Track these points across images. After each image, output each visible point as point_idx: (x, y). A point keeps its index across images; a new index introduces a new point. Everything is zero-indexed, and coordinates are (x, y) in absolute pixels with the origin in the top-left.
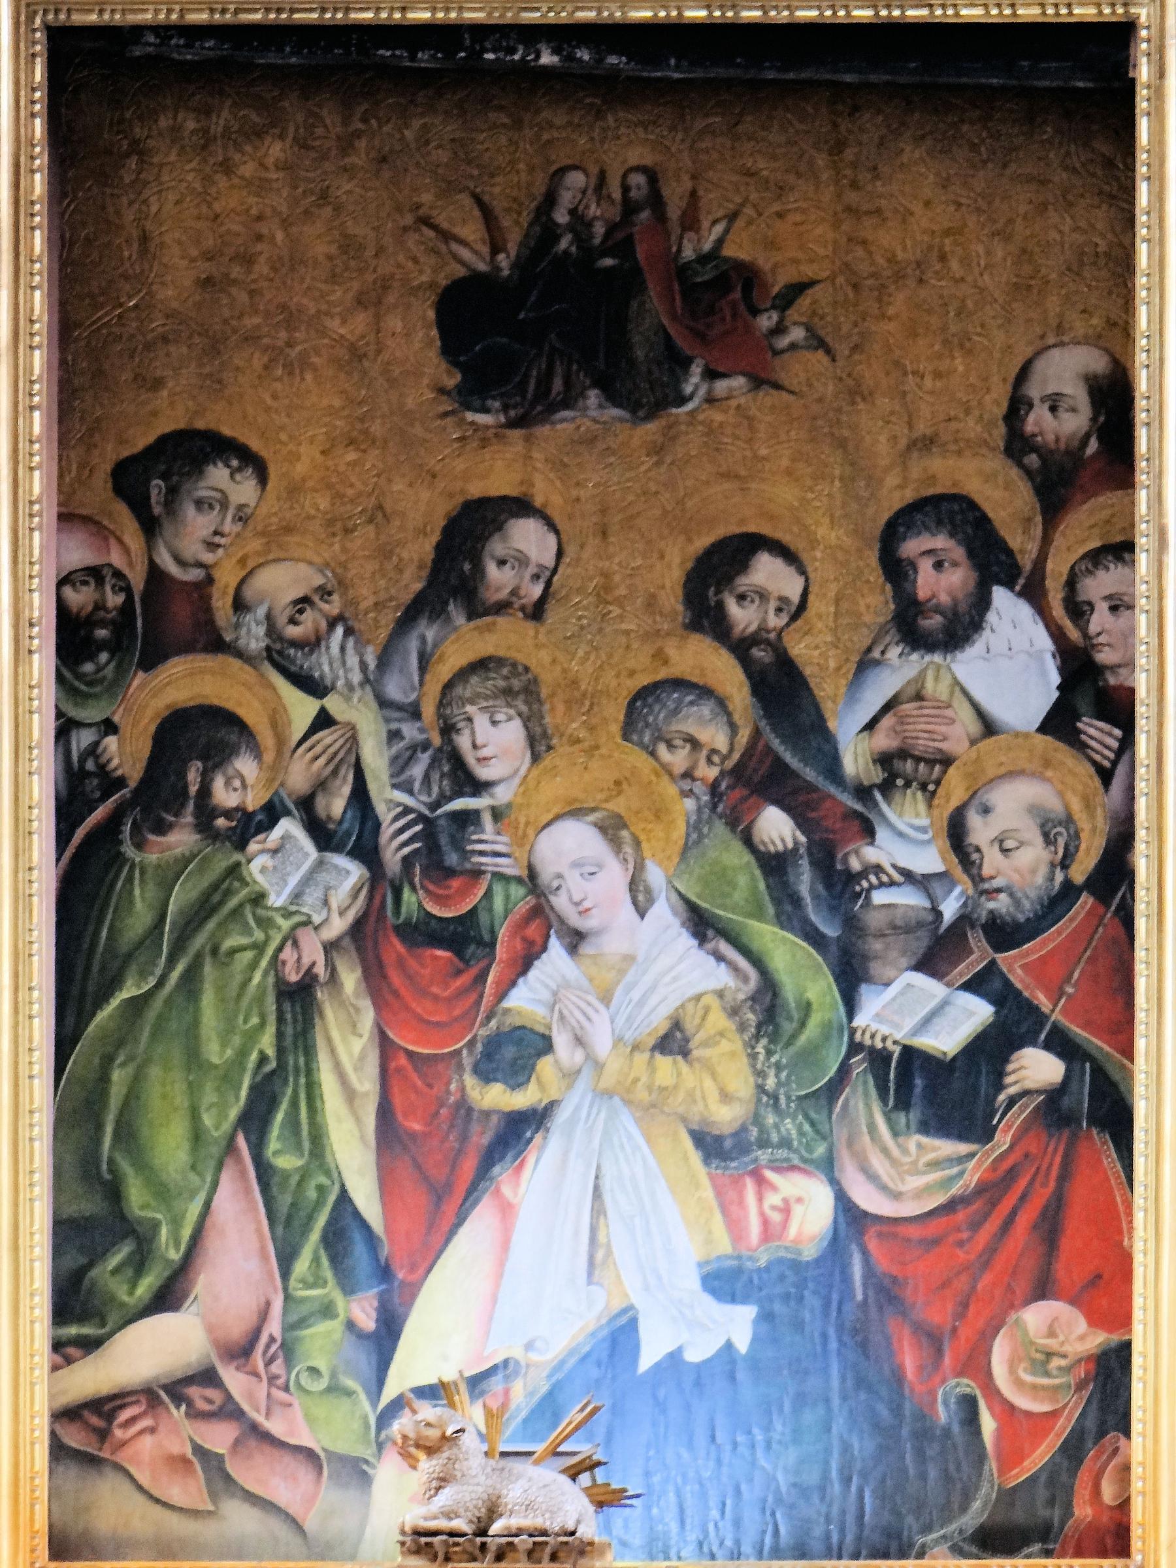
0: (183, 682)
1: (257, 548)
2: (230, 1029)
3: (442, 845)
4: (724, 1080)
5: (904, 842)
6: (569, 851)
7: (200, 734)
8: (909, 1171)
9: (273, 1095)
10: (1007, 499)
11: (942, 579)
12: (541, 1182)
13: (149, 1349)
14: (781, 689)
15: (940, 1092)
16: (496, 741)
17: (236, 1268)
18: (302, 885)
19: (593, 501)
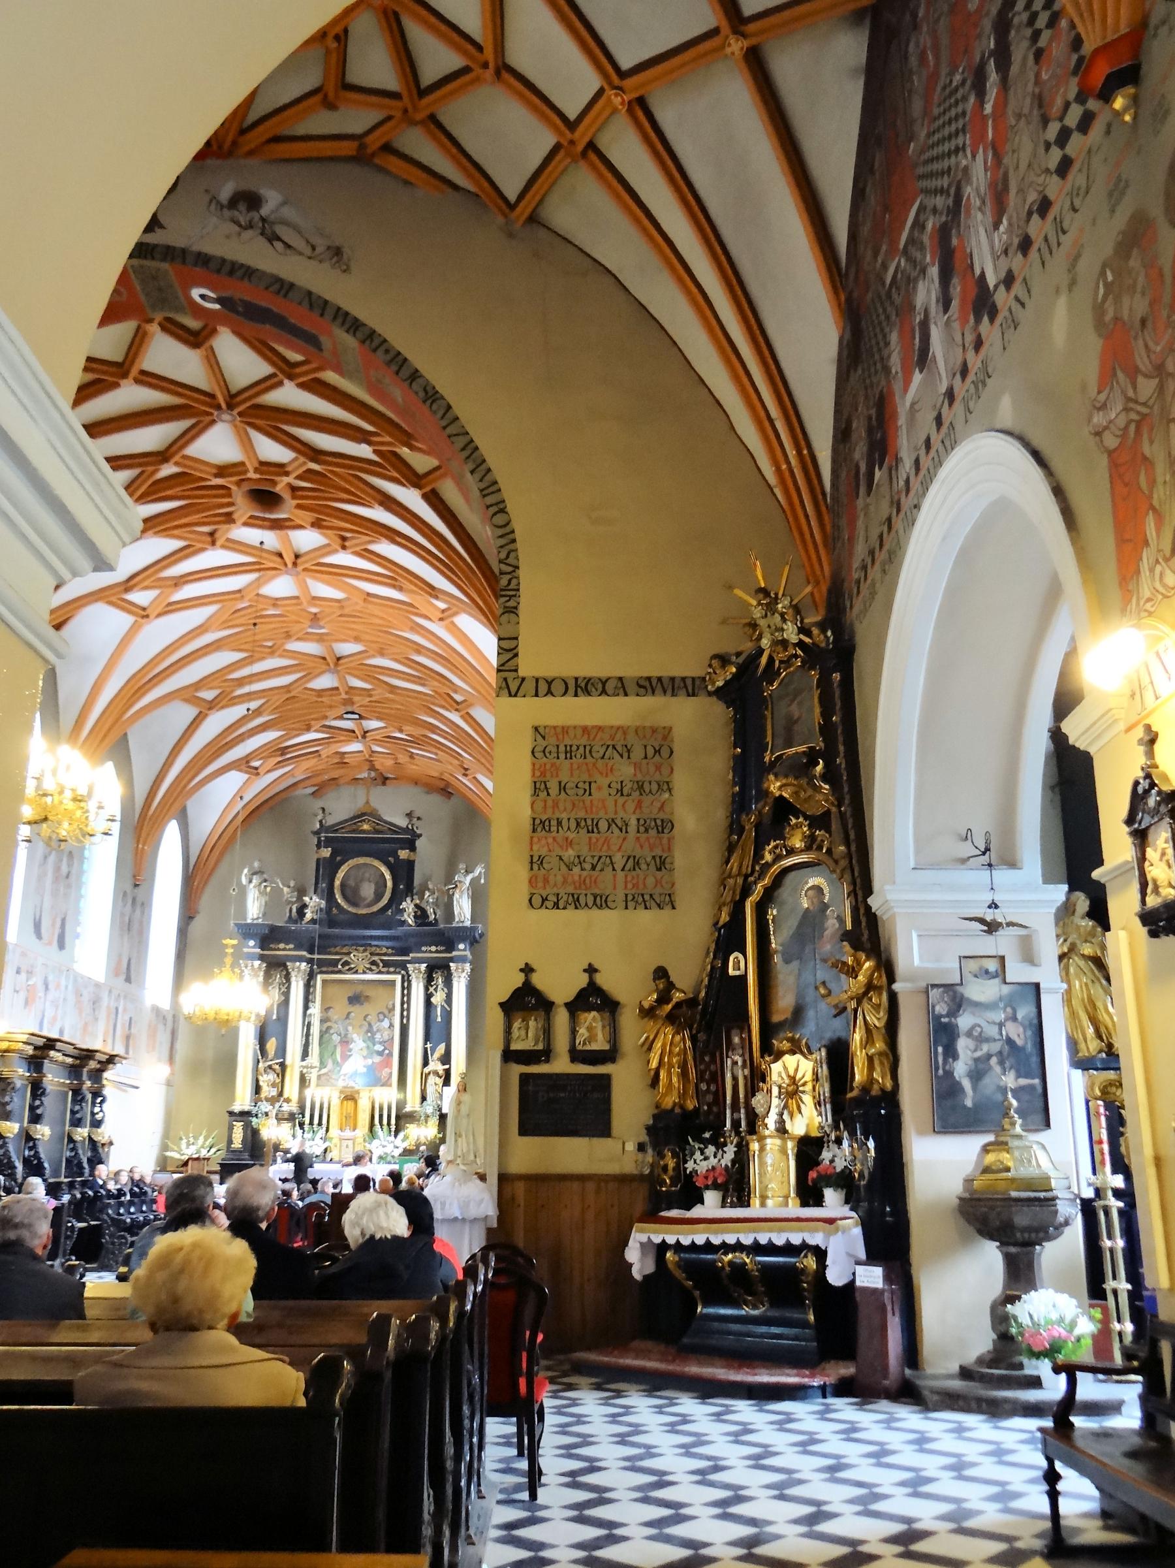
0: (329, 1024)
1: (334, 1015)
2: (330, 1048)
3: (346, 1035)
4: (365, 1053)
5: (378, 1036)
6: (355, 1036)
7: (329, 1028)
8: (377, 1059)
9: (333, 1053)
10: (386, 1012)
11: (381, 1017)
12: (351, 1059)
13: (324, 1071)
14: (370, 1025)
15: (380, 1053)
16: (350, 1028)
17: (330, 1065)
18: (336, 1038)
19: (357, 1011)
